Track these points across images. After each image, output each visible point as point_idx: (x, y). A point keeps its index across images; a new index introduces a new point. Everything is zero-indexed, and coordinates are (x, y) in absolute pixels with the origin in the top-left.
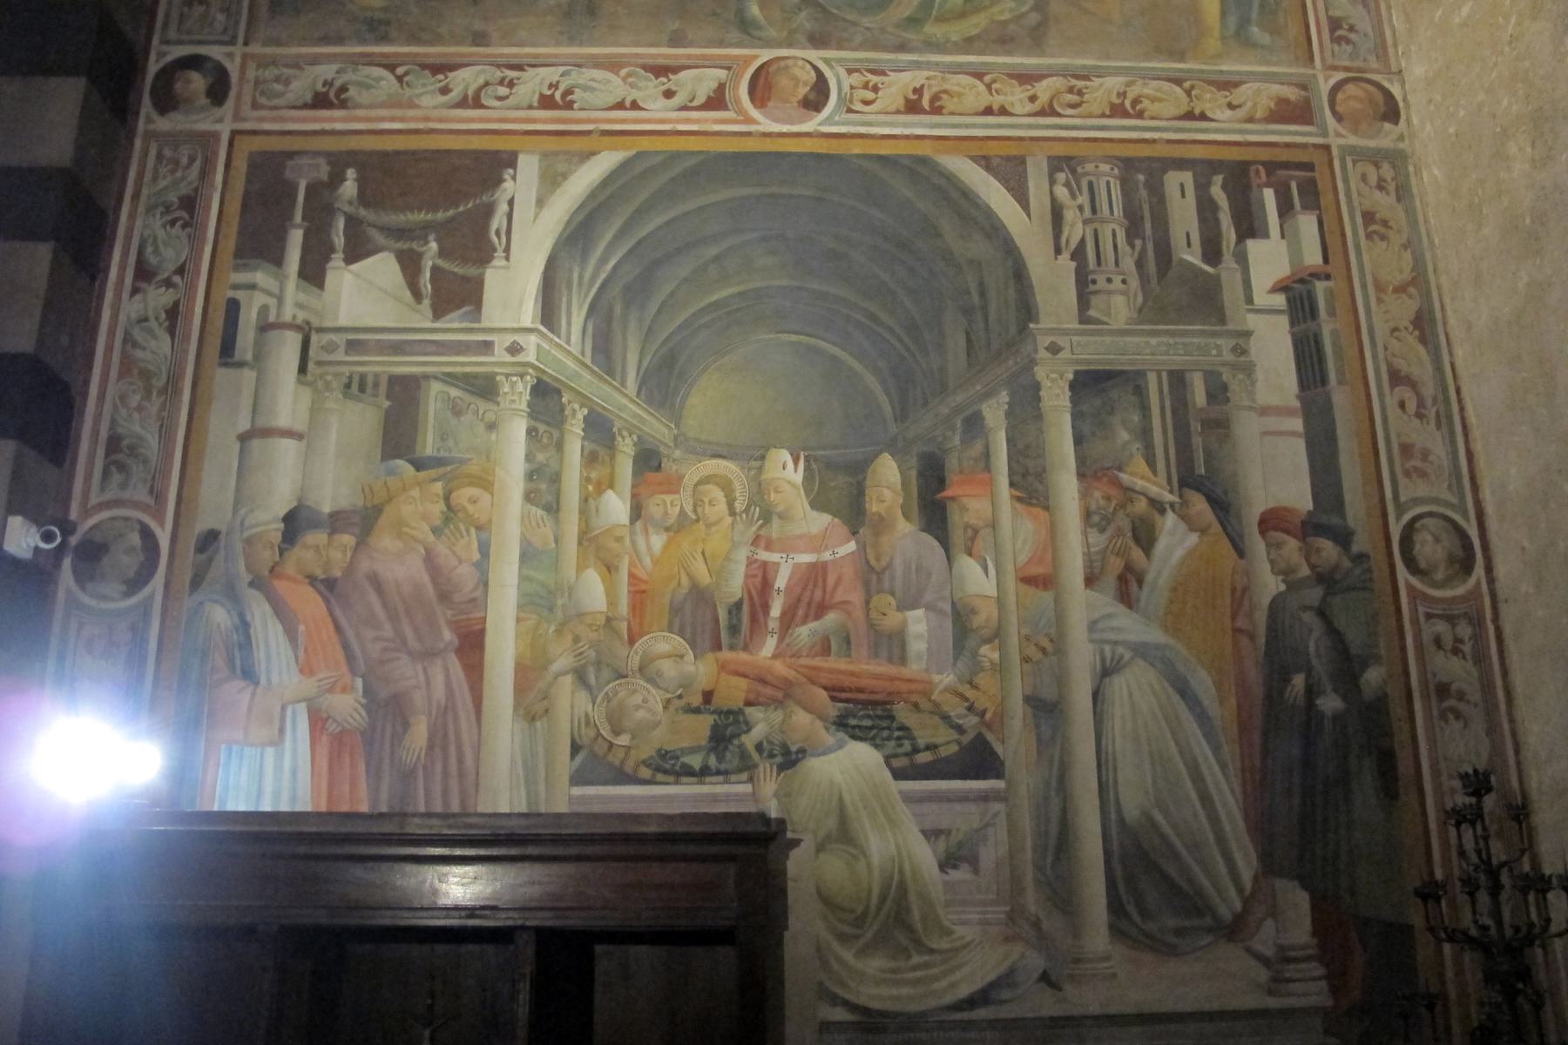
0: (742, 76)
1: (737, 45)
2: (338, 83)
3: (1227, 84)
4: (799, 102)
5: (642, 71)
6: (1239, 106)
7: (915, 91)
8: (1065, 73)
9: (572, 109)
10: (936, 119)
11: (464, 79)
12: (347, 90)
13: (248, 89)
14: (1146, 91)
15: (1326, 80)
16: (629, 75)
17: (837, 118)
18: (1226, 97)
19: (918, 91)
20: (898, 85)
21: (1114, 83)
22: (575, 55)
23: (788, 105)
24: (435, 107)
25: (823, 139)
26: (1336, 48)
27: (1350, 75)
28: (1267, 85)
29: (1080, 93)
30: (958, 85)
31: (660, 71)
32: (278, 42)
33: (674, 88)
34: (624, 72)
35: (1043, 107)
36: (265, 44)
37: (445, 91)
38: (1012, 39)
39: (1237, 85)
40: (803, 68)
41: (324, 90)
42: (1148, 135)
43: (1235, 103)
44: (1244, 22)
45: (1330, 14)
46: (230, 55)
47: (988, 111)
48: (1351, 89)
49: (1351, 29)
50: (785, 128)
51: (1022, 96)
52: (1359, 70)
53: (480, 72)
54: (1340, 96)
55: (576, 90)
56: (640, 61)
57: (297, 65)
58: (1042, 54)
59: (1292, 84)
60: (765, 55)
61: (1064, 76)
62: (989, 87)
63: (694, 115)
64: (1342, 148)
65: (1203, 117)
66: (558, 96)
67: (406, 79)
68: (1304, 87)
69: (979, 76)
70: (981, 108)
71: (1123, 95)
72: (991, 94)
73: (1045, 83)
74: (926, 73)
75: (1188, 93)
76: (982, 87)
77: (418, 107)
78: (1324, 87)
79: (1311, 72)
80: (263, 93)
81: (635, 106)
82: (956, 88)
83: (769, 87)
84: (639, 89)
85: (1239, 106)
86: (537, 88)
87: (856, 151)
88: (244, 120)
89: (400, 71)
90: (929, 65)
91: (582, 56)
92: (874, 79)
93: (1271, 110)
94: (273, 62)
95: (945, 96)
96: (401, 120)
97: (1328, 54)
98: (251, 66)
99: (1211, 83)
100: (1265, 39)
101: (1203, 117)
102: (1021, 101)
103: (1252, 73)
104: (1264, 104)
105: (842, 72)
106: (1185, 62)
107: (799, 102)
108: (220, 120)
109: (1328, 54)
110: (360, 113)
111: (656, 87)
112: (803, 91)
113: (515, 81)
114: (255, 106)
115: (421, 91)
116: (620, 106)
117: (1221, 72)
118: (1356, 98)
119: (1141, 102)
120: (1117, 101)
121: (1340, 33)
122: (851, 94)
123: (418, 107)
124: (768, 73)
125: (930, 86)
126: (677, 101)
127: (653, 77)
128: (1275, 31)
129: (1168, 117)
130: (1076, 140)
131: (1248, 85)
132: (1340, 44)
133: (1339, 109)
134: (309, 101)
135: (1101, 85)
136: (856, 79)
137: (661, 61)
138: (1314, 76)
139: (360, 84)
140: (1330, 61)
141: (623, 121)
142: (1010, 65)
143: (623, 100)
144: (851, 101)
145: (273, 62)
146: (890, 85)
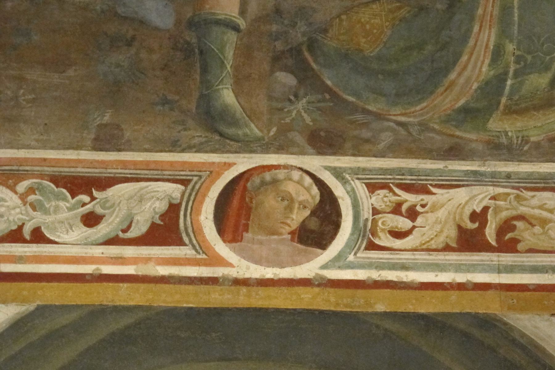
0: (204, 196)
1: (199, 149)
7: (474, 216)
17: (351, 258)
23: (275, 237)
25: (332, 290)
30: (541, 207)
34: (22, 187)
40: (300, 182)
50: (269, 273)
63: (130, 251)
74: (492, 190)
82: (537, 212)
84: (46, 212)
87: (380, 308)
92: (410, 199)
95: (520, 224)
105: (361, 190)
107: (292, 233)
111: (70, 209)
124: (245, 188)
125: (497, 210)
127: (68, 194)
137: (81, 170)
141: (20, 259)
143: (20, 228)
144: (374, 233)
146: (434, 208)
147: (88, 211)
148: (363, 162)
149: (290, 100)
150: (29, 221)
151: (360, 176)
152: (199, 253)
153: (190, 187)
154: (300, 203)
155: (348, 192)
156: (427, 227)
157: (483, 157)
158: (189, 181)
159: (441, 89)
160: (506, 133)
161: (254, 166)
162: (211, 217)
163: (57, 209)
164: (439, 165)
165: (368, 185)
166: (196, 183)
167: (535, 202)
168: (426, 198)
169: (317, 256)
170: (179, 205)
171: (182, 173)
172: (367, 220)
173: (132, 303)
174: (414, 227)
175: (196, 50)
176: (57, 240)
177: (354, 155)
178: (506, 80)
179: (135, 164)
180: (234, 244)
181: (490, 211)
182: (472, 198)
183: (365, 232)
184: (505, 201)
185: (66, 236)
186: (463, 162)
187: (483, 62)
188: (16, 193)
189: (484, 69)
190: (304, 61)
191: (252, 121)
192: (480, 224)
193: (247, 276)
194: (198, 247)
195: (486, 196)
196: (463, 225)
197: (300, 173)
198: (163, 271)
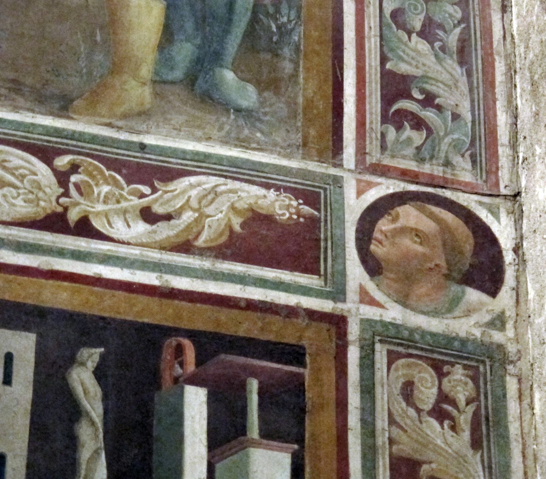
6: (168, 217)
15: (360, 193)
18: (142, 196)
26: (392, 133)
27: (413, 188)
52: (432, 182)
59: (287, 189)
79: (333, 171)
85: (168, 217)
103: (207, 157)
117: (143, 147)
118: (417, 233)
131: (193, 179)
132: (399, 128)
138: (337, 181)
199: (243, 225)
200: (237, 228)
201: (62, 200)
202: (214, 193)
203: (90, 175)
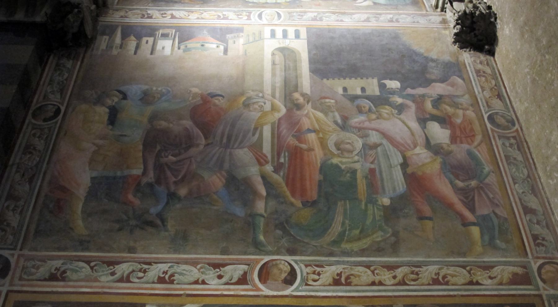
0: (255, 269)
2: (62, 269)
3: (488, 267)
4: (282, 281)
5: (208, 266)
6: (495, 277)
7: (338, 275)
8: (409, 264)
9: (173, 284)
10: (348, 288)
11: (122, 269)
12: (66, 272)
13: (19, 271)
14: (449, 272)
15: (535, 264)
16: (201, 268)
17: (300, 288)
18: (488, 273)
19: (340, 275)
20: (330, 272)
21: (433, 269)
22: (176, 258)
23: (277, 282)
24: (107, 282)
26: (538, 249)
27: (546, 261)
28: (507, 267)
29: (417, 274)
30: (358, 271)
31: (216, 266)
32: (36, 250)
33: (222, 274)
34: (199, 267)
35: (400, 281)
36: (30, 250)
37: (113, 274)
38: (383, 249)
39: (493, 267)
40: (284, 265)
41: (55, 272)
42: (452, 293)
43: (492, 276)
44: (492, 238)
45: (532, 233)
46: (13, 255)
47: (373, 284)
48: (547, 267)
49: (544, 239)
50: (275, 293)
51: (389, 276)
52: (550, 258)
53: (130, 265)
54: (543, 271)
55: (176, 274)
56: (207, 261)
57: (43, 260)
58: (397, 256)
60: (266, 259)
61: (409, 266)
62: (373, 272)
63: (232, 287)
64: (547, 295)
65: (478, 283)
66: (167, 277)
67: (95, 268)
68: (525, 267)
69: (368, 267)
70: (370, 282)
71: (438, 274)
72: (374, 275)
73: (400, 270)
75: (469, 272)
76: (369, 272)
77: (99, 281)
78: (535, 267)
79: (527, 260)
80: (25, 273)
81: (204, 282)
82: (357, 273)
83: (268, 273)
84: (206, 274)
85: (495, 277)
86: (157, 273)
88: (14, 285)
89: (92, 264)
90: (343, 263)
91: (179, 259)
92: (318, 269)
93: (510, 279)
94: (32, 259)
95: (352, 277)
96: (91, 287)
97: (534, 252)
98: (22, 260)
99: (480, 267)
100: (503, 245)
101: (478, 283)
102: (389, 278)
103: (499, 262)
104: (506, 276)
105: (303, 266)
106: (466, 258)
107: (282, 281)
108: (3, 285)
109: (534, 252)
110: (71, 283)
111: (214, 274)
112: (284, 276)
113: (147, 270)
114: (21, 279)
115: (102, 273)
116: (196, 282)
117: (484, 262)
119: (447, 277)
120: (436, 277)
121: (538, 241)
122: (307, 276)
123: (99, 281)
125: (345, 273)
126: (224, 280)
127: (213, 269)
128: (507, 242)
129: (460, 284)
130: (417, 296)
132: (539, 247)
133: (543, 277)
134: (47, 278)
135: (427, 270)
136: (309, 269)
138: (529, 262)
139: (73, 270)
140: (535, 255)
141: (198, 290)
142: (383, 261)
143: (198, 280)
144: (307, 280)
145: (32, 259)
146: (326, 272)
147: (219, 274)
148: (303, 258)
149: (281, 239)
150: (201, 277)
151: (302, 262)
152: (253, 287)
153: (250, 266)
154: (285, 271)
155: (299, 267)
156: (324, 278)
157: (339, 256)
158: (250, 264)
159: (326, 235)
160: (347, 248)
161: (269, 260)
162: (257, 275)
163: (209, 274)
164: (326, 259)
165: (305, 265)
166: (252, 265)
167: (356, 270)
168: (323, 269)
169: (290, 288)
170: (247, 272)
171: (248, 262)
172: (305, 276)
173: (233, 303)
174: (319, 278)
175: (252, 223)
176: (209, 283)
177: (301, 256)
178: (346, 232)
179: (233, 259)
180: (264, 284)
181: (343, 273)
182: (337, 269)
183: (304, 280)
184: (347, 270)
185: (212, 282)
186: (334, 258)
187: (339, 226)
188: (197, 269)
189: (339, 229)
190: (285, 227)
191: (269, 245)
192: (340, 277)
193: (268, 294)
194: (253, 285)
195: (341, 268)
196: (334, 277)
197: (284, 261)
198: (243, 293)
199: (512, 276)
200: (511, 277)
201: (471, 277)
202: (503, 270)
203: (475, 270)
